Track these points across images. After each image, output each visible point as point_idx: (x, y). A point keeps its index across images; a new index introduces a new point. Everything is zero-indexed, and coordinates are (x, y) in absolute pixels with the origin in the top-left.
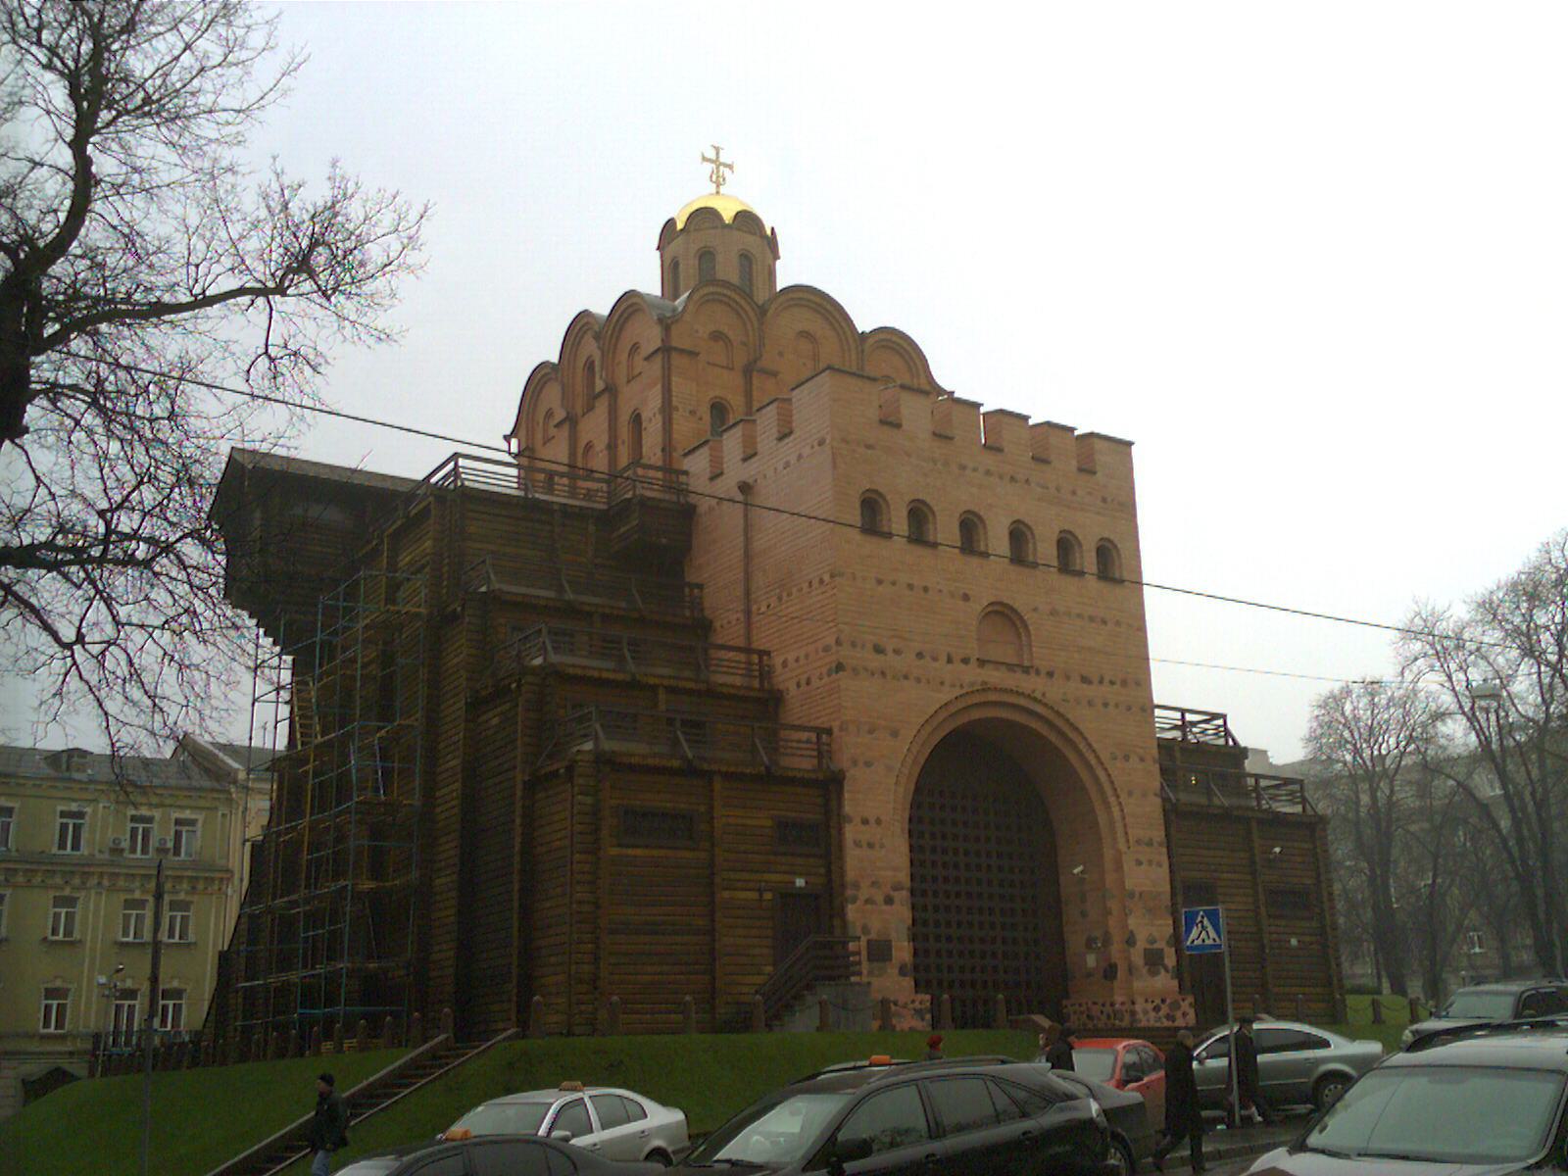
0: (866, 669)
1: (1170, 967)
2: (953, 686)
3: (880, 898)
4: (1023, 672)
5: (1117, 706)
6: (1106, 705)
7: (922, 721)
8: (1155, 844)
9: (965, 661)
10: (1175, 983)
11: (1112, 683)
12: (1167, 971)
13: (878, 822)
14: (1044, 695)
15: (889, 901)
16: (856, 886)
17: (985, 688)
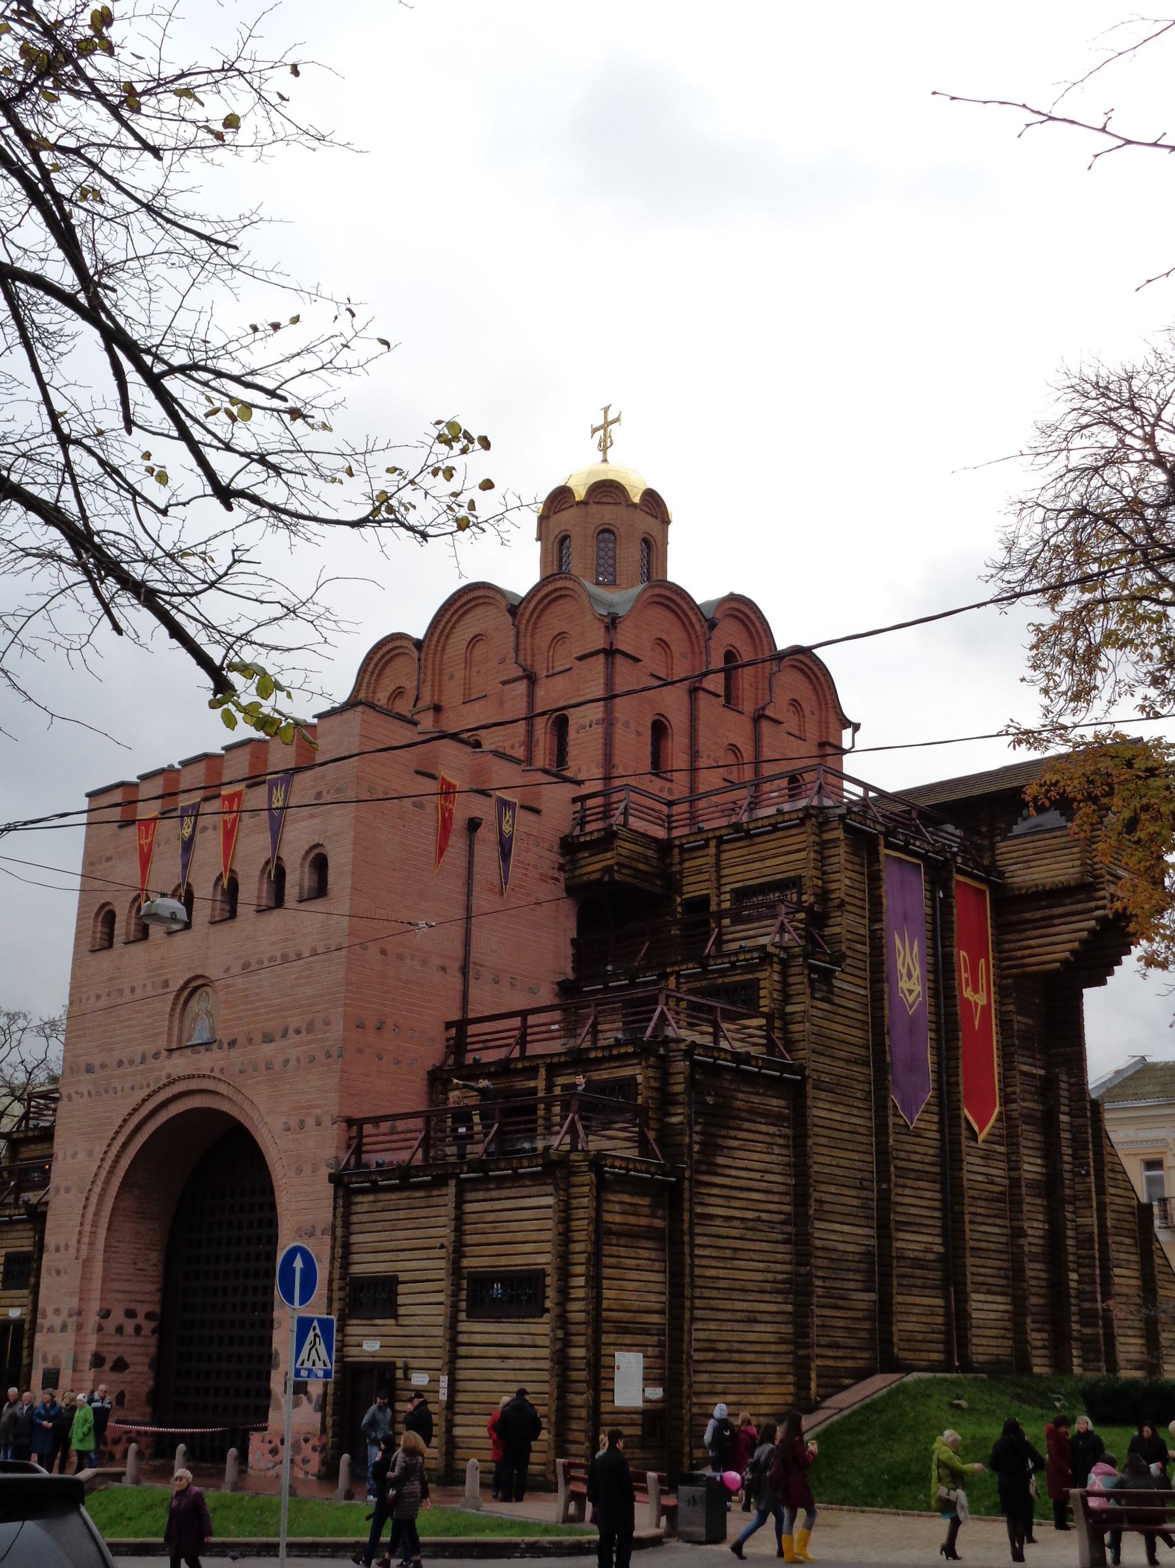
0: (77, 1093)
1: (314, 1397)
2: (141, 1088)
3: (58, 1327)
4: (207, 1050)
5: (298, 1061)
6: (287, 1061)
7: (111, 1134)
8: (318, 1232)
9: (156, 1056)
10: (319, 1415)
11: (298, 1032)
12: (310, 1400)
13: (67, 1248)
14: (222, 1070)
15: (64, 1328)
16: (44, 1316)
17: (172, 1082)
